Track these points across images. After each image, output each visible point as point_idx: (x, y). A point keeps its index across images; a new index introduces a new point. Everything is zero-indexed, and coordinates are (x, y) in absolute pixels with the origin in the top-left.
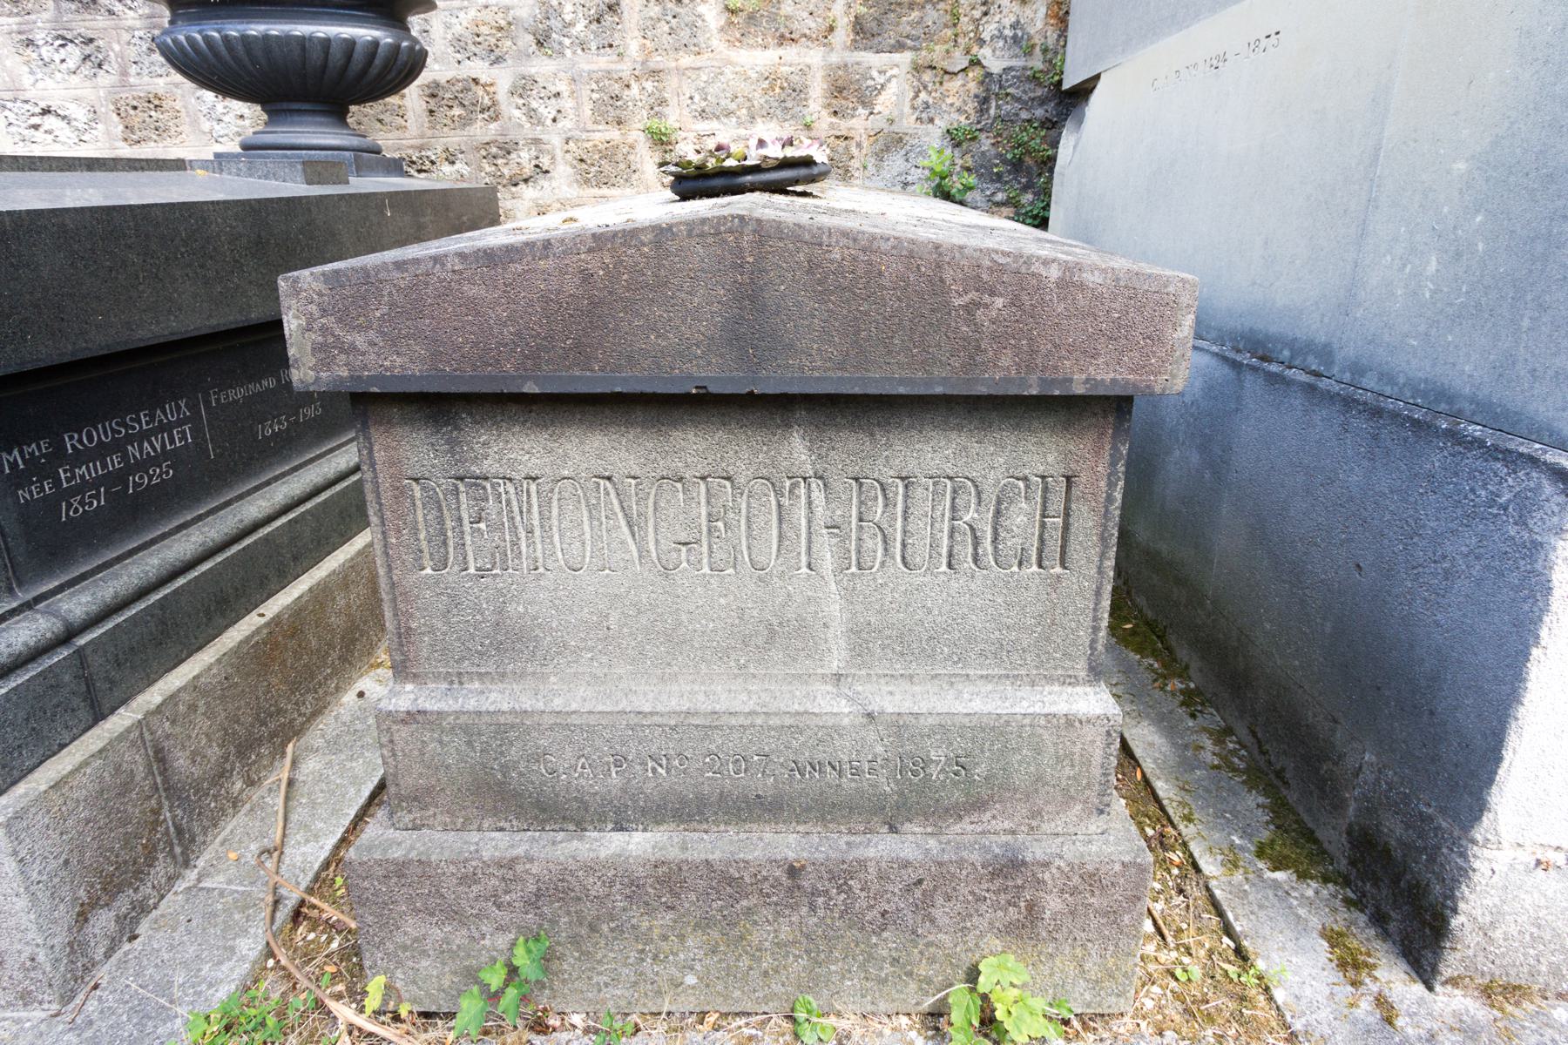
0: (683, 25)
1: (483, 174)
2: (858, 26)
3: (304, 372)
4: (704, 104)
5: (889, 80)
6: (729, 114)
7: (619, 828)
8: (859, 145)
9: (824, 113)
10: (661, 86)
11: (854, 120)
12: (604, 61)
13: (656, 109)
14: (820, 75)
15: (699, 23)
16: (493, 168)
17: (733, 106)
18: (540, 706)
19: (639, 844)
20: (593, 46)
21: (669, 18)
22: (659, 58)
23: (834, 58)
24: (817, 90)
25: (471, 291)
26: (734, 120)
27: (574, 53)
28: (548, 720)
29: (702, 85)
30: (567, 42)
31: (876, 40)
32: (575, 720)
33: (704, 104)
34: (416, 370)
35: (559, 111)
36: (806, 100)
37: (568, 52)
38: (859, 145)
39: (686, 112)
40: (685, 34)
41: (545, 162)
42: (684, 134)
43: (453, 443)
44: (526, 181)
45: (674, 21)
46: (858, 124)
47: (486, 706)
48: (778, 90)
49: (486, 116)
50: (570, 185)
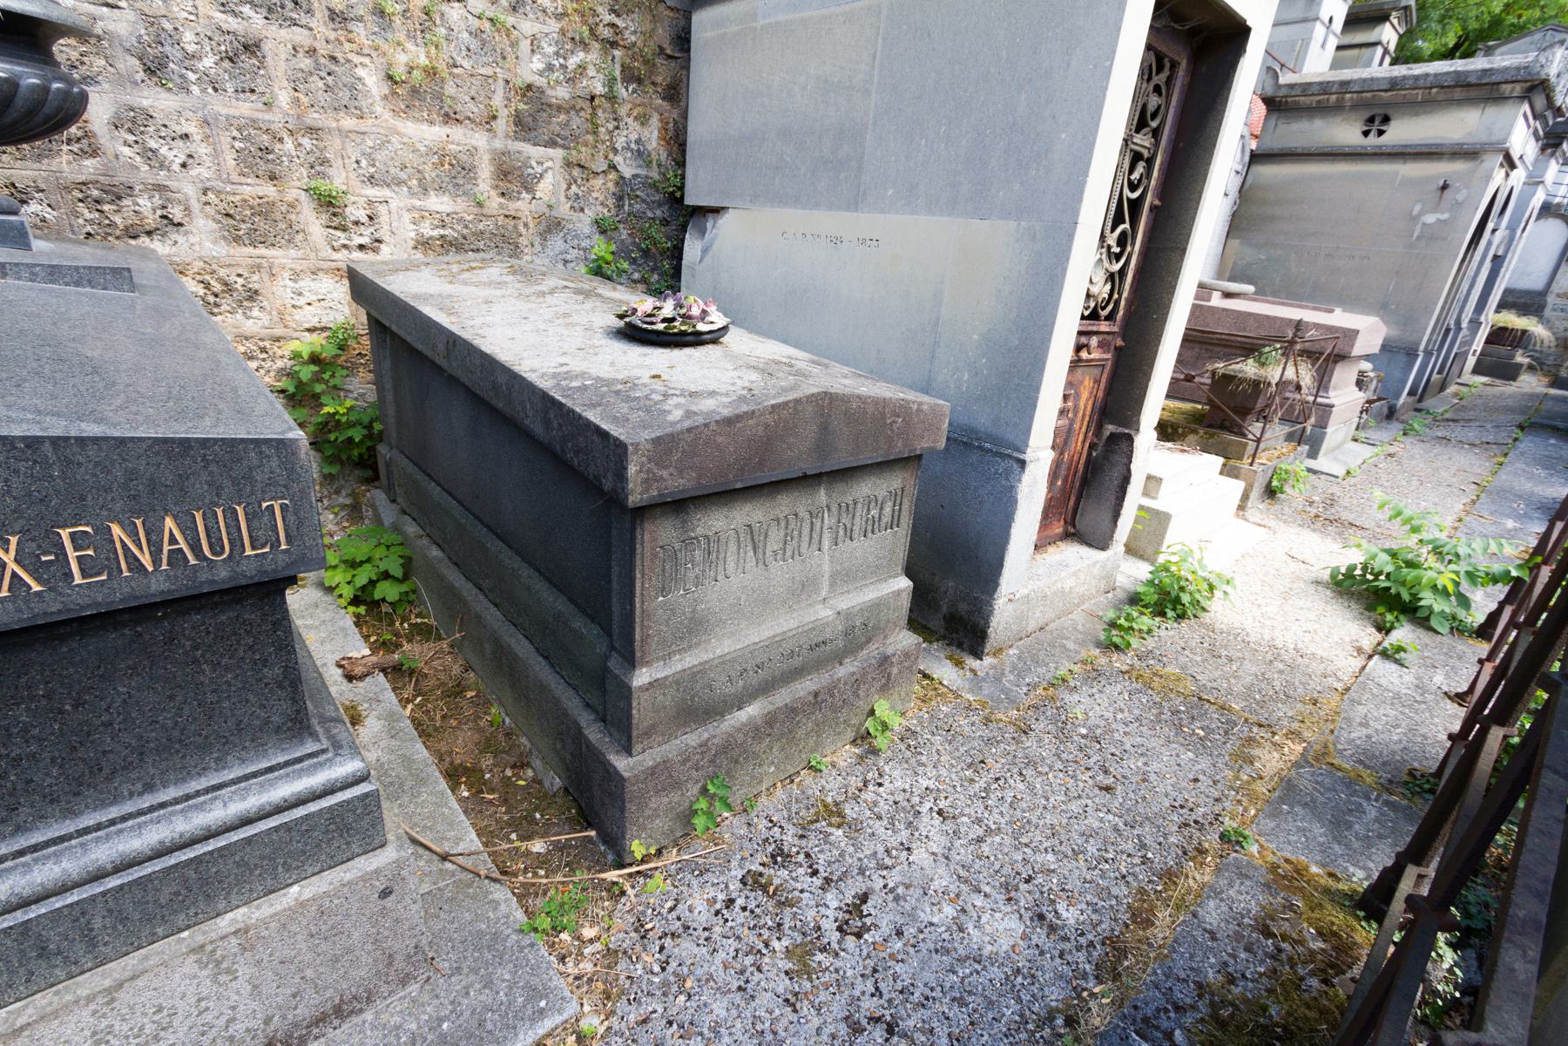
0: (340, 85)
1: (81, 221)
2: (518, 120)
3: (635, 498)
4: (372, 170)
5: (546, 171)
6: (400, 183)
7: (740, 709)
8: (526, 225)
9: (493, 193)
10: (321, 145)
11: (520, 203)
12: (245, 108)
13: (317, 168)
14: (486, 157)
15: (360, 87)
16: (97, 215)
17: (403, 176)
18: (712, 656)
19: (753, 711)
20: (230, 88)
21: (323, 74)
22: (316, 115)
23: (498, 144)
24: (485, 172)
25: (720, 439)
26: (405, 189)
27: (204, 91)
28: (716, 662)
29: (369, 150)
30: (192, 76)
31: (533, 134)
32: (728, 657)
33: (372, 170)
34: (689, 485)
35: (190, 156)
36: (476, 179)
37: (195, 89)
38: (526, 225)
39: (352, 175)
40: (344, 95)
41: (176, 213)
42: (353, 199)
43: (684, 522)
44: (149, 233)
45: (330, 79)
46: (523, 206)
47: (687, 666)
48: (447, 166)
49: (75, 147)
50: (215, 242)
